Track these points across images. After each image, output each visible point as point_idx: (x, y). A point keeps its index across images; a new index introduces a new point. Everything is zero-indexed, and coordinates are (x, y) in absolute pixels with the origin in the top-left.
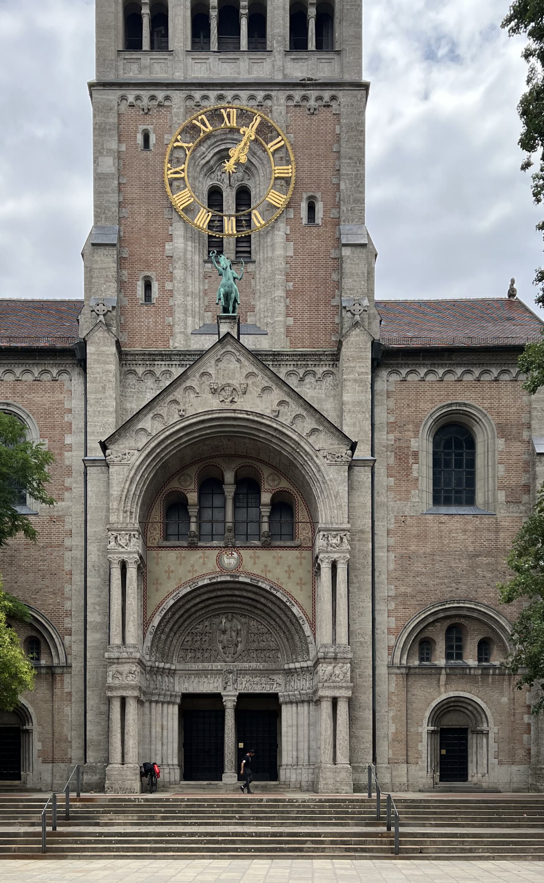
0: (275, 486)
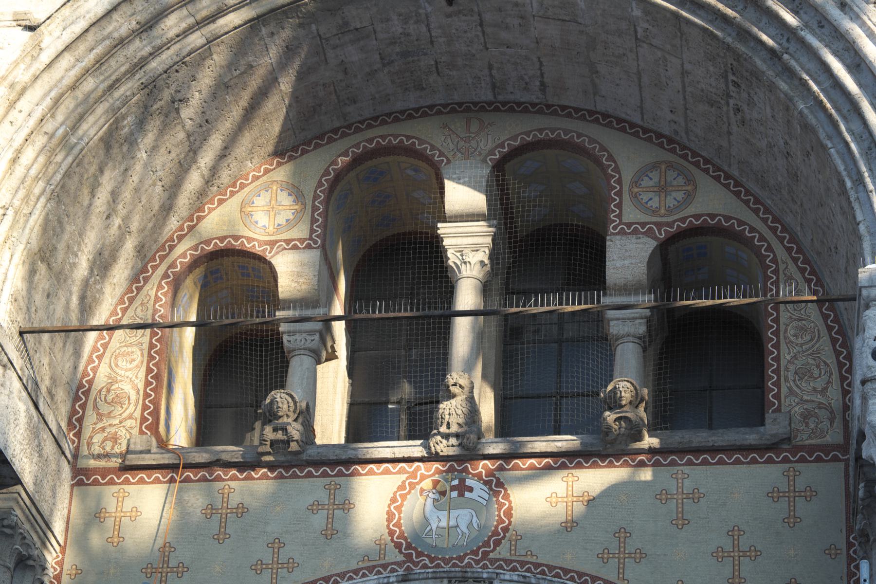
0: (670, 211)
